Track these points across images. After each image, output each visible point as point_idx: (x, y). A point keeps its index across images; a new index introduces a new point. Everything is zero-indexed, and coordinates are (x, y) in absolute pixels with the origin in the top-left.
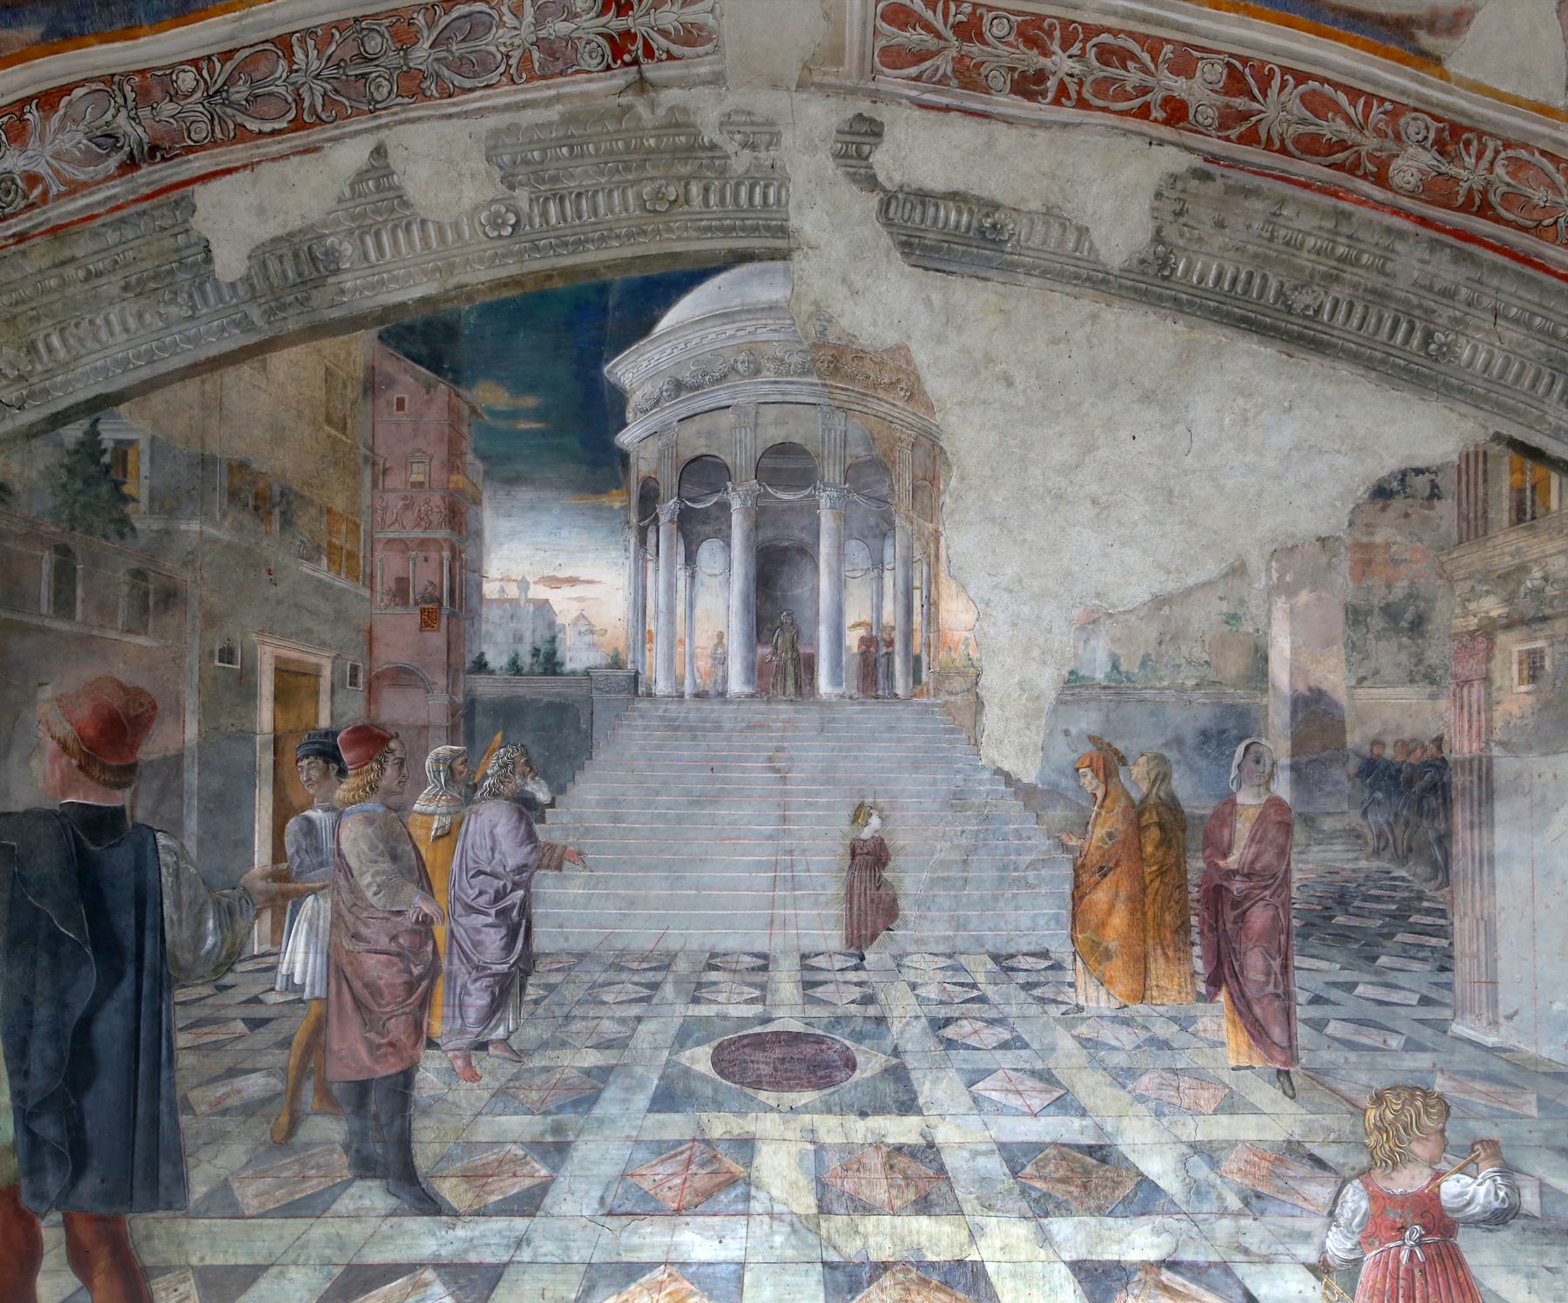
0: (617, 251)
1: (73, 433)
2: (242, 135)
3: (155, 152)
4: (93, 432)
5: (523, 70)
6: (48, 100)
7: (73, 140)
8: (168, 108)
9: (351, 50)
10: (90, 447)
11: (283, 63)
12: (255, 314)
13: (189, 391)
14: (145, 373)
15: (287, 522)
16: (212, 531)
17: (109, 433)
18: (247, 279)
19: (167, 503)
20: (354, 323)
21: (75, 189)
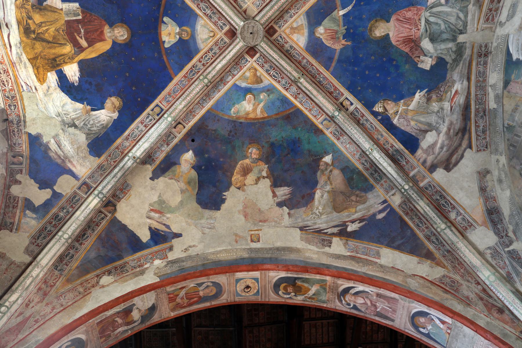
0: (504, 58)
1: (505, 130)
2: (485, 102)
3: (484, 112)
4: (505, 127)
5: (486, 68)
6: (476, 122)
7: (481, 121)
8: (480, 109)
9: (479, 88)
10: (507, 128)
11: (479, 96)
12: (500, 104)
13: (505, 114)
14: (502, 119)
15: (519, 106)
16: (517, 116)
17: (506, 125)
18: (497, 104)
19: (513, 121)
20: (503, 93)
21: (486, 122)
